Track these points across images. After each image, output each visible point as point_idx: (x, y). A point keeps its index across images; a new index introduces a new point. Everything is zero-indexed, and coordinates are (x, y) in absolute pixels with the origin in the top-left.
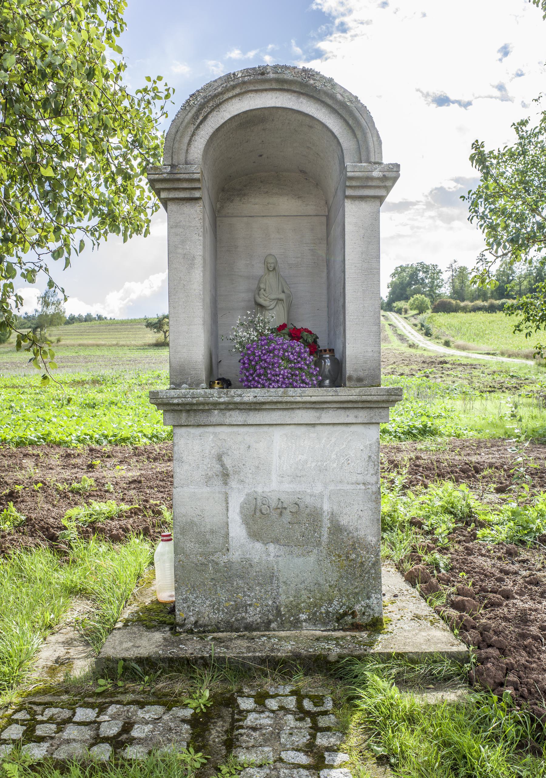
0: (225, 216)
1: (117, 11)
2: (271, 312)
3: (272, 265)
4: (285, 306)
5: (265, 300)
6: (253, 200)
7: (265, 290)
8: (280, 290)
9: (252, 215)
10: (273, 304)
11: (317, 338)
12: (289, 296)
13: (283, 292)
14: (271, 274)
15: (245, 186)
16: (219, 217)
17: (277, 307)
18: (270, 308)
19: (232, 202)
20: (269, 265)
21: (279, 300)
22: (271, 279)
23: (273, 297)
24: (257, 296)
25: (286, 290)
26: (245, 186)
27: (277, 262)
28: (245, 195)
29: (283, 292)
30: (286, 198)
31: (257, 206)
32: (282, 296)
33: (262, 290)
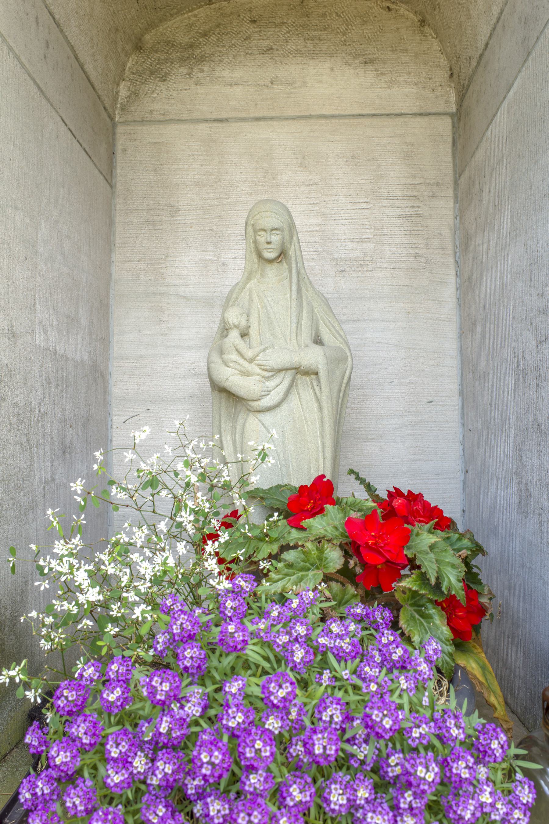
0: (143, 122)
1: (418, 199)
2: (266, 418)
3: (275, 238)
4: (324, 397)
5: (245, 374)
6: (226, 73)
7: (244, 335)
8: (306, 336)
9: (224, 115)
10: (278, 387)
11: (478, 550)
12: (338, 360)
13: (318, 341)
14: (272, 271)
15: (205, 35)
16: (125, 123)
17: (294, 401)
18: (266, 402)
19: (163, 79)
20: (262, 239)
21: (301, 372)
22: (272, 292)
23: (276, 359)
24: (216, 358)
25: (326, 336)
26: (205, 35)
27: (292, 227)
28: (202, 59)
29: (318, 341)
30: (327, 65)
31: (238, 90)
32: (314, 357)
33: (234, 335)
